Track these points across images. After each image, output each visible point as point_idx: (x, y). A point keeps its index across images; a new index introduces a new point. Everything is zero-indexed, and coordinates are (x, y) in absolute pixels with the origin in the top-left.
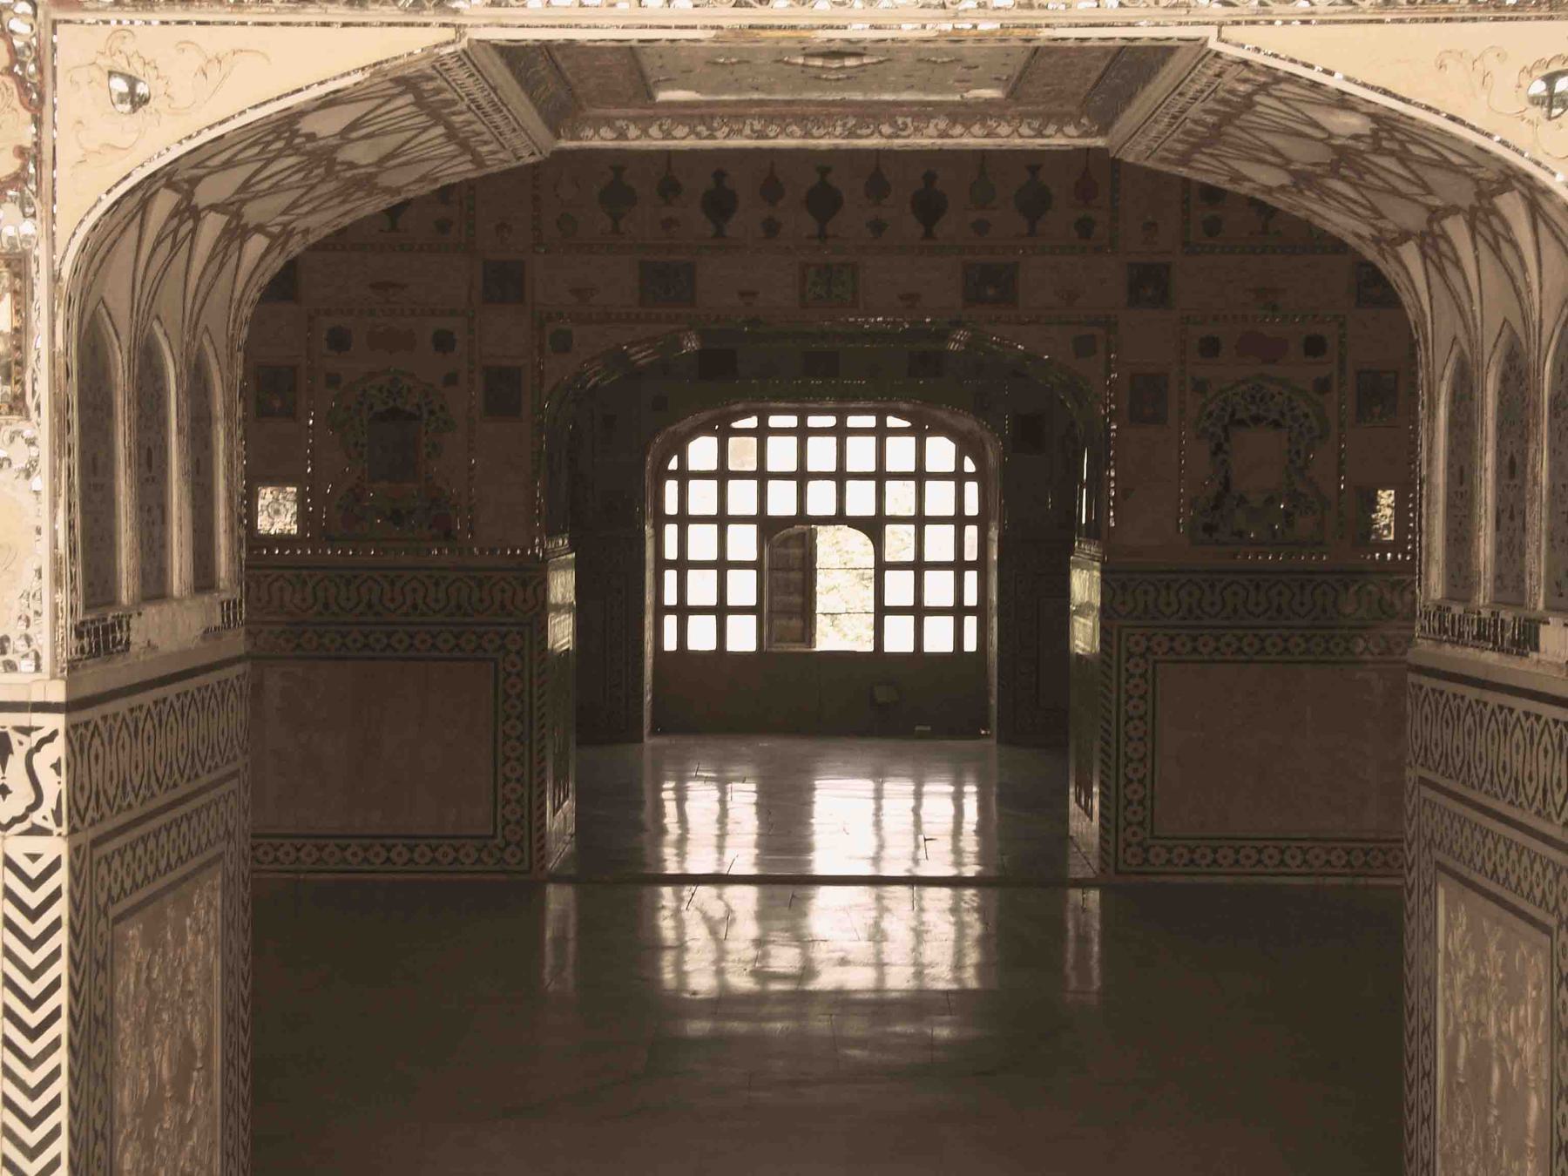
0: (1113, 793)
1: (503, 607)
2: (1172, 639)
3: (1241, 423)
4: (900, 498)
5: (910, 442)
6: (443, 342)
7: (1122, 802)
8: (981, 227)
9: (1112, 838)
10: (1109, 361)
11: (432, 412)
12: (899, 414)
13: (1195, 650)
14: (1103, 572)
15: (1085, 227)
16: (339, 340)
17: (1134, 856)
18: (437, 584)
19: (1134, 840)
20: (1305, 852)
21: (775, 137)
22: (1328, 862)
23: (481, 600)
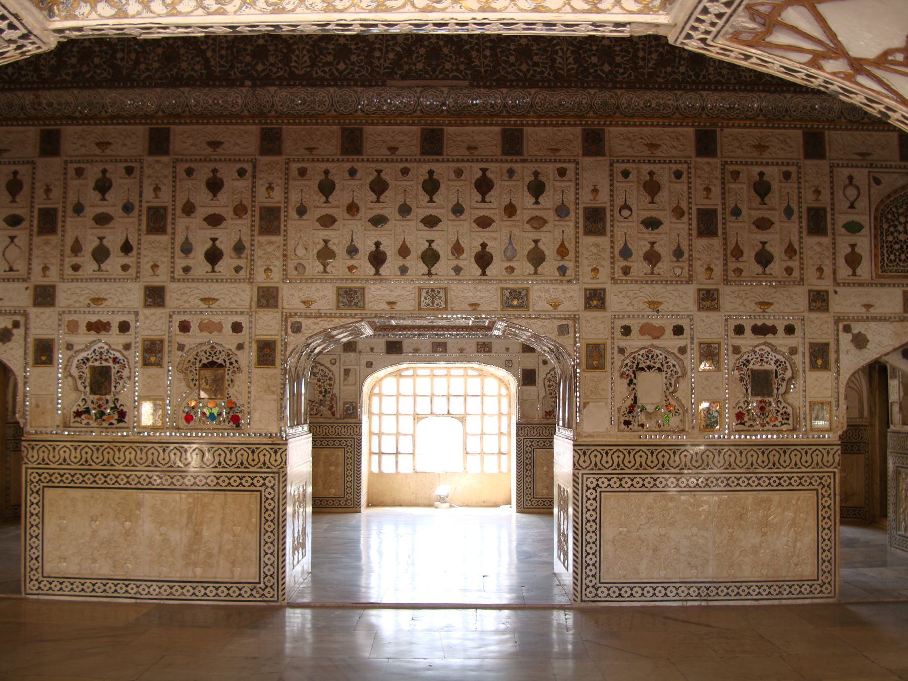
0: (579, 561)
1: (264, 464)
2: (609, 480)
3: (642, 369)
4: (474, 405)
5: (478, 380)
6: (237, 328)
7: (584, 565)
8: (511, 270)
9: (579, 583)
10: (575, 337)
11: (231, 363)
12: (472, 368)
13: (621, 485)
14: (574, 445)
15: (562, 270)
16: (185, 327)
17: (590, 592)
18: (231, 451)
19: (590, 585)
20: (677, 589)
21: (293, 11)
22: (688, 594)
23: (253, 460)
